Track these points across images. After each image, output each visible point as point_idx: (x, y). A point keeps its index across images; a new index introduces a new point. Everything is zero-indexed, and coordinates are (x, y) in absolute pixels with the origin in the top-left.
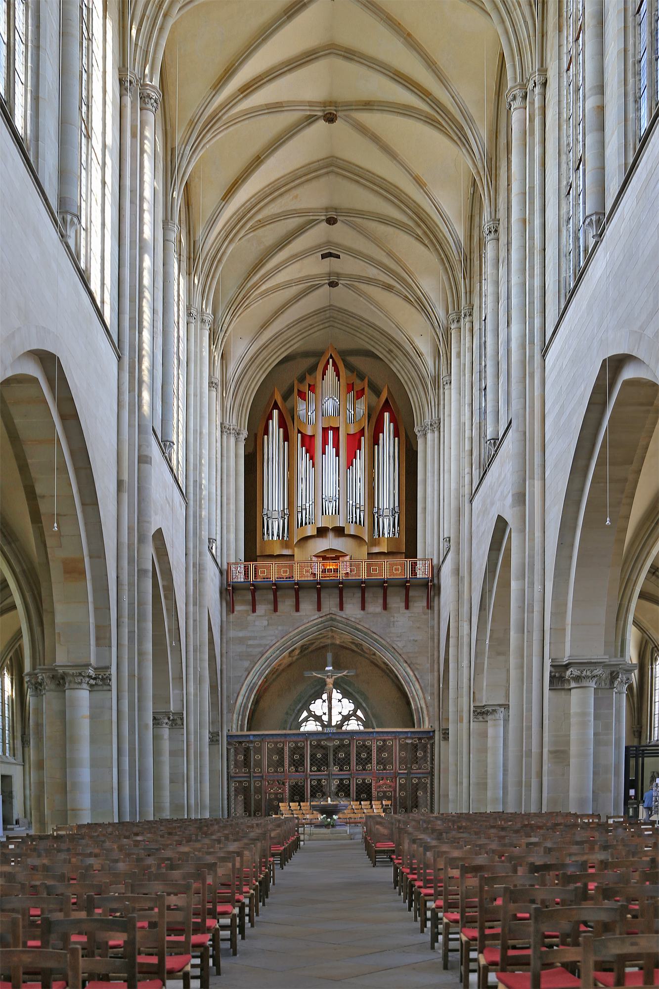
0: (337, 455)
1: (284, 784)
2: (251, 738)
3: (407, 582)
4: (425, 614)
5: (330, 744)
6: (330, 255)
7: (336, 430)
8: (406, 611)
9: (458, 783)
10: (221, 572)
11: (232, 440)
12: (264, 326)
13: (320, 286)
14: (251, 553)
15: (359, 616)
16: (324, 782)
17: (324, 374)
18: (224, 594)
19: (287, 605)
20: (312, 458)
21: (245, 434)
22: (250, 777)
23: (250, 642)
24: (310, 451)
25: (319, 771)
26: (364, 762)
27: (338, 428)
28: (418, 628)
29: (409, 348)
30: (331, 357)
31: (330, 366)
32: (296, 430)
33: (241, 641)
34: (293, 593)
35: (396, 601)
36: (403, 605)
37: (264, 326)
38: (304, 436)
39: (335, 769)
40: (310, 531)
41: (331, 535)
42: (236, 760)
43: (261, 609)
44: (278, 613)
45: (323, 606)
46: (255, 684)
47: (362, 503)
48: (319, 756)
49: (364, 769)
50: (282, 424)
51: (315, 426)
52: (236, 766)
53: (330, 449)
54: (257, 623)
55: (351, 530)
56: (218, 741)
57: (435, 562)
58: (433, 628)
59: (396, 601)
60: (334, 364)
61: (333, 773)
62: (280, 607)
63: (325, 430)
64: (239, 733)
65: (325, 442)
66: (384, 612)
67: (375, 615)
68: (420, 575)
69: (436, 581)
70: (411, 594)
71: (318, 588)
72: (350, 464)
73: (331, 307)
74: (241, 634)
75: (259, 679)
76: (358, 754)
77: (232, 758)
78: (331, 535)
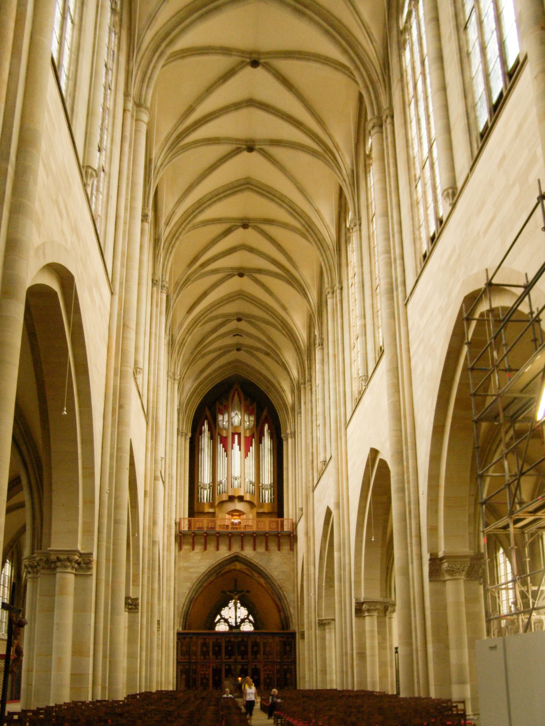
3: (279, 533)
4: (289, 554)
6: (237, 335)
8: (279, 552)
9: (310, 670)
28: (286, 563)
35: (273, 546)
36: (276, 548)
51: (227, 430)
57: (294, 521)
58: (293, 563)
59: (273, 546)
66: (267, 552)
68: (286, 529)
69: (295, 533)
70: (282, 540)
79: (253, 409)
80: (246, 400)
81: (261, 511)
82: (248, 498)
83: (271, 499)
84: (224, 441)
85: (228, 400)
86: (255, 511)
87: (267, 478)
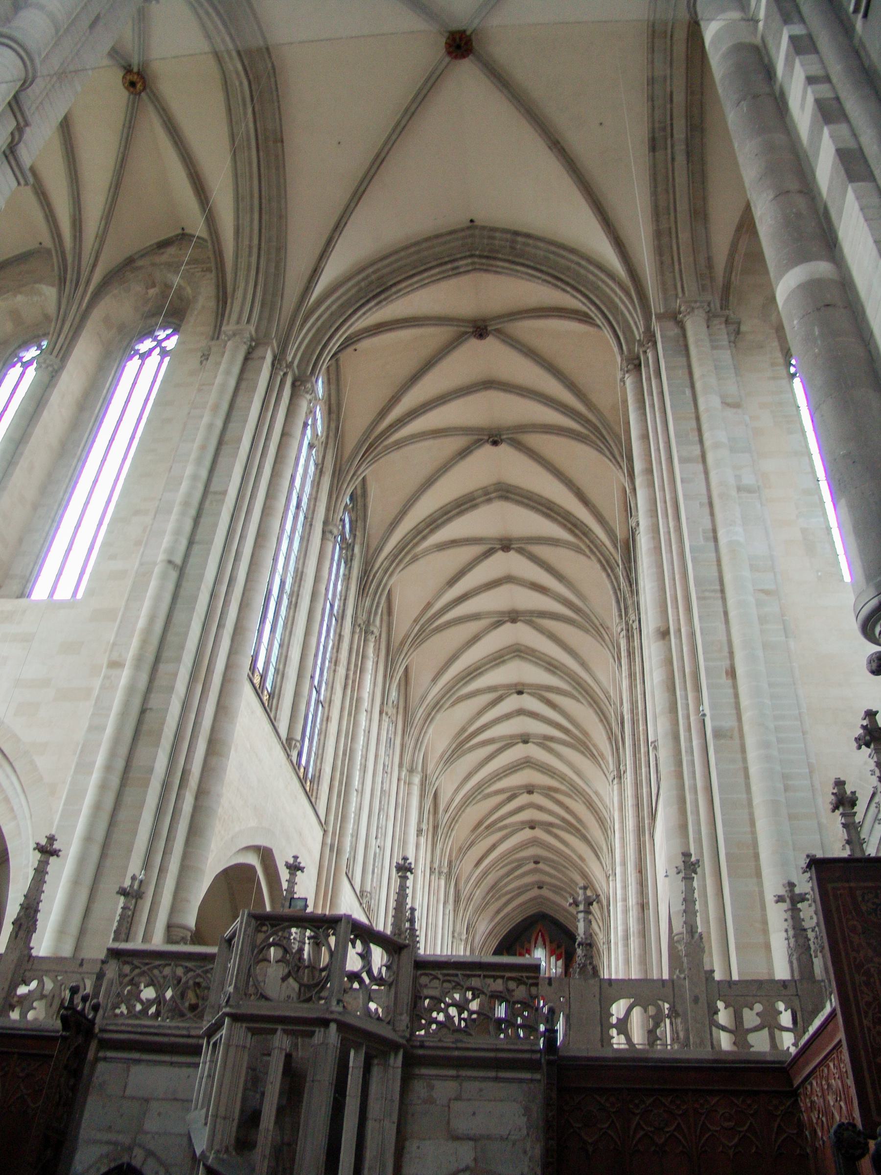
31: (540, 939)
60: (543, 936)
73: (541, 896)
79: (561, 954)
80: (551, 942)
85: (530, 942)
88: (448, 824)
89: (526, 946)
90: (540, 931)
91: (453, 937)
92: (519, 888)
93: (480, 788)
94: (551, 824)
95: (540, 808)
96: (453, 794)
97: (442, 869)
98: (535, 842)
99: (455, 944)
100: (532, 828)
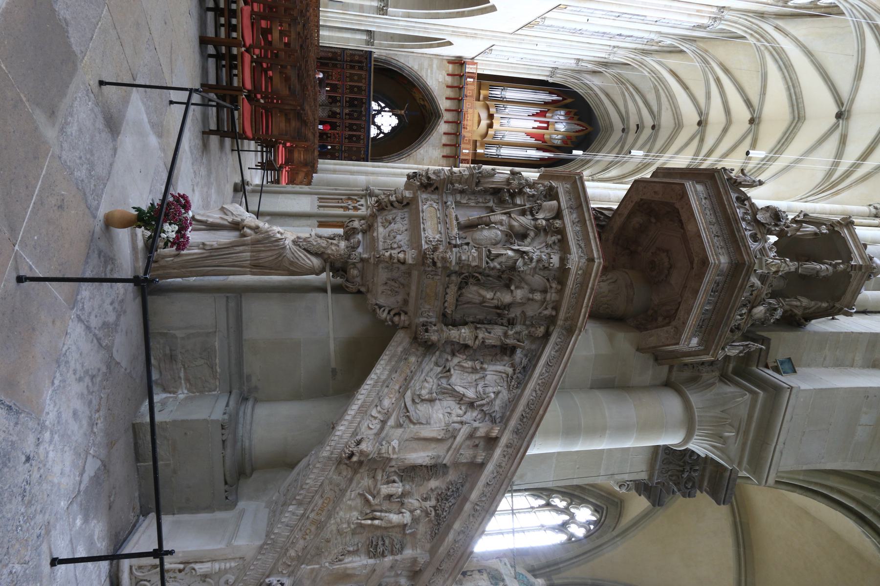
0: (533, 128)
1: (339, 81)
2: (369, 65)
5: (363, 109)
7: (547, 128)
8: (441, 156)
10: (473, 58)
11: (548, 74)
12: (607, 95)
13: (624, 125)
14: (481, 77)
15: (440, 131)
16: (338, 104)
17: (578, 125)
18: (458, 59)
19: (450, 93)
20: (533, 115)
21: (551, 80)
22: (344, 61)
23: (429, 71)
24: (537, 115)
25: (346, 102)
26: (350, 127)
27: (548, 129)
29: (586, 167)
30: (587, 129)
31: (581, 128)
32: (549, 108)
33: (431, 66)
34: (457, 96)
35: (447, 151)
36: (445, 154)
37: (607, 95)
38: (546, 112)
39: (347, 111)
40: (492, 110)
41: (488, 122)
42: (355, 55)
43: (449, 80)
44: (445, 87)
45: (448, 112)
46: (403, 71)
47: (505, 139)
48: (356, 102)
49: (346, 127)
50: (554, 102)
52: (352, 55)
53: (537, 124)
54: (440, 76)
55: (491, 132)
56: (368, 45)
59: (447, 151)
60: (582, 130)
61: (344, 110)
62: (449, 89)
63: (548, 123)
64: (373, 59)
65: (541, 122)
67: (441, 139)
71: (458, 112)
72: (528, 134)
74: (435, 66)
75: (406, 74)
76: (355, 124)
77: (356, 52)
78: (488, 122)
80: (576, 137)
81: (478, 144)
82: (491, 132)
83: (488, 154)
84: (542, 114)
86: (478, 139)
87: (506, 152)
88: (760, 30)
89: (576, 117)
90: (587, 129)
91: (614, 47)
92: (627, 112)
93: (786, 67)
94: (702, 140)
95: (725, 130)
96: (793, 36)
97: (718, 22)
98: (678, 125)
99: (608, 48)
100: (700, 123)
